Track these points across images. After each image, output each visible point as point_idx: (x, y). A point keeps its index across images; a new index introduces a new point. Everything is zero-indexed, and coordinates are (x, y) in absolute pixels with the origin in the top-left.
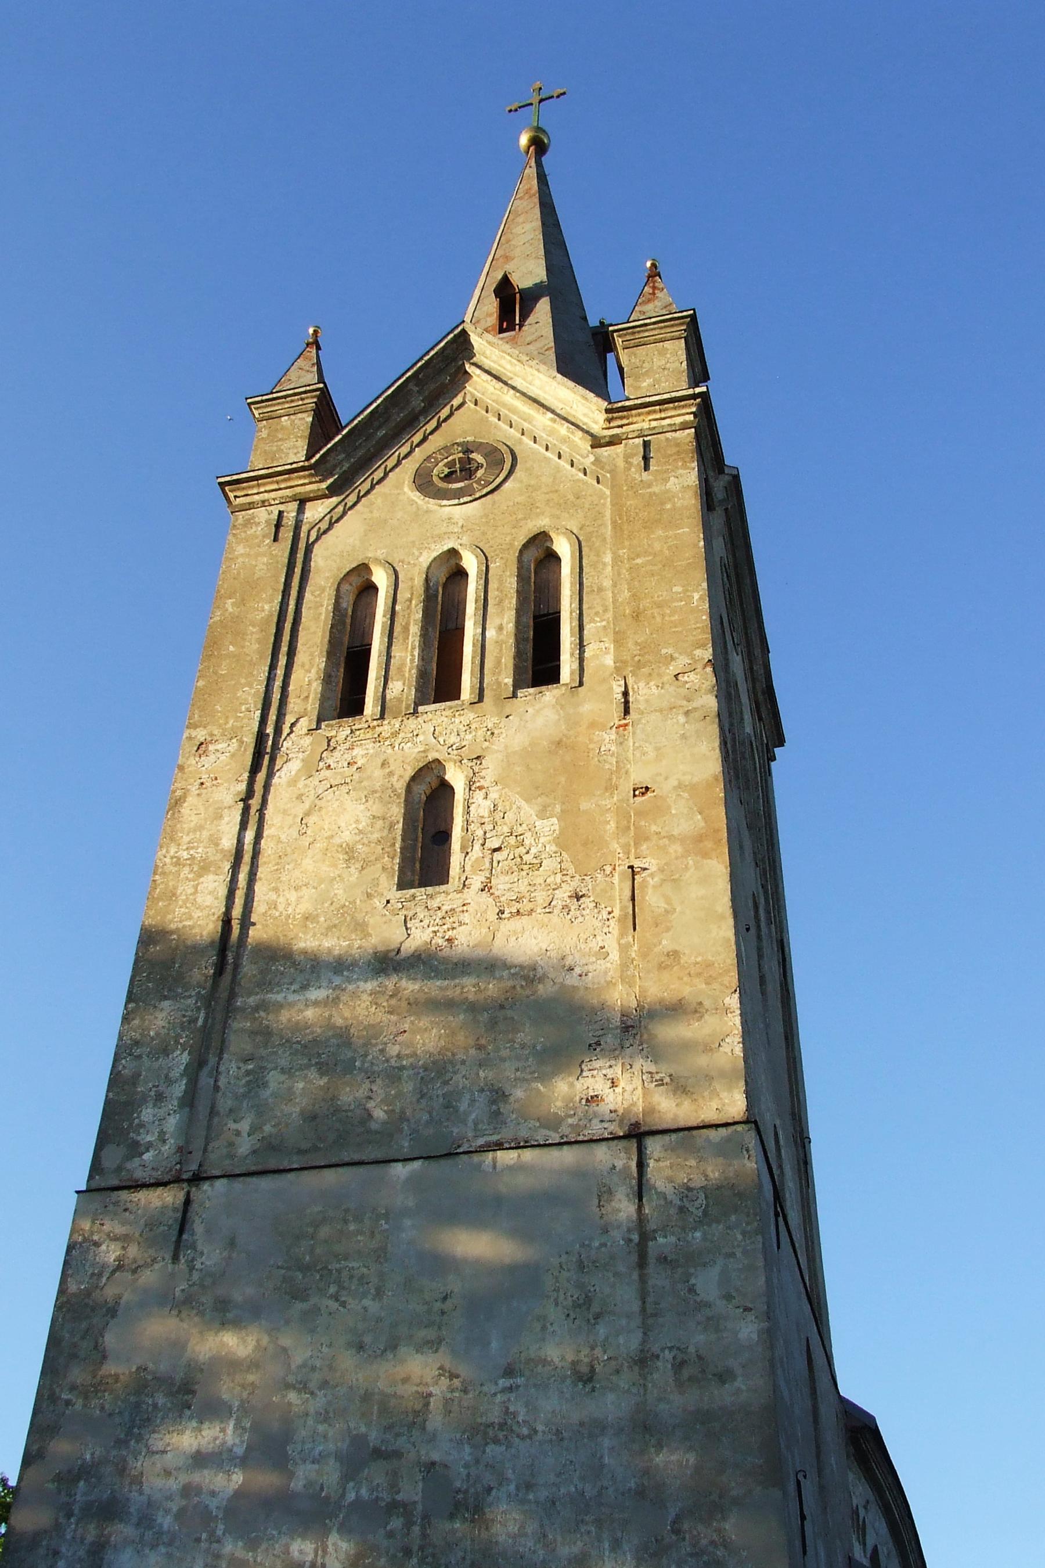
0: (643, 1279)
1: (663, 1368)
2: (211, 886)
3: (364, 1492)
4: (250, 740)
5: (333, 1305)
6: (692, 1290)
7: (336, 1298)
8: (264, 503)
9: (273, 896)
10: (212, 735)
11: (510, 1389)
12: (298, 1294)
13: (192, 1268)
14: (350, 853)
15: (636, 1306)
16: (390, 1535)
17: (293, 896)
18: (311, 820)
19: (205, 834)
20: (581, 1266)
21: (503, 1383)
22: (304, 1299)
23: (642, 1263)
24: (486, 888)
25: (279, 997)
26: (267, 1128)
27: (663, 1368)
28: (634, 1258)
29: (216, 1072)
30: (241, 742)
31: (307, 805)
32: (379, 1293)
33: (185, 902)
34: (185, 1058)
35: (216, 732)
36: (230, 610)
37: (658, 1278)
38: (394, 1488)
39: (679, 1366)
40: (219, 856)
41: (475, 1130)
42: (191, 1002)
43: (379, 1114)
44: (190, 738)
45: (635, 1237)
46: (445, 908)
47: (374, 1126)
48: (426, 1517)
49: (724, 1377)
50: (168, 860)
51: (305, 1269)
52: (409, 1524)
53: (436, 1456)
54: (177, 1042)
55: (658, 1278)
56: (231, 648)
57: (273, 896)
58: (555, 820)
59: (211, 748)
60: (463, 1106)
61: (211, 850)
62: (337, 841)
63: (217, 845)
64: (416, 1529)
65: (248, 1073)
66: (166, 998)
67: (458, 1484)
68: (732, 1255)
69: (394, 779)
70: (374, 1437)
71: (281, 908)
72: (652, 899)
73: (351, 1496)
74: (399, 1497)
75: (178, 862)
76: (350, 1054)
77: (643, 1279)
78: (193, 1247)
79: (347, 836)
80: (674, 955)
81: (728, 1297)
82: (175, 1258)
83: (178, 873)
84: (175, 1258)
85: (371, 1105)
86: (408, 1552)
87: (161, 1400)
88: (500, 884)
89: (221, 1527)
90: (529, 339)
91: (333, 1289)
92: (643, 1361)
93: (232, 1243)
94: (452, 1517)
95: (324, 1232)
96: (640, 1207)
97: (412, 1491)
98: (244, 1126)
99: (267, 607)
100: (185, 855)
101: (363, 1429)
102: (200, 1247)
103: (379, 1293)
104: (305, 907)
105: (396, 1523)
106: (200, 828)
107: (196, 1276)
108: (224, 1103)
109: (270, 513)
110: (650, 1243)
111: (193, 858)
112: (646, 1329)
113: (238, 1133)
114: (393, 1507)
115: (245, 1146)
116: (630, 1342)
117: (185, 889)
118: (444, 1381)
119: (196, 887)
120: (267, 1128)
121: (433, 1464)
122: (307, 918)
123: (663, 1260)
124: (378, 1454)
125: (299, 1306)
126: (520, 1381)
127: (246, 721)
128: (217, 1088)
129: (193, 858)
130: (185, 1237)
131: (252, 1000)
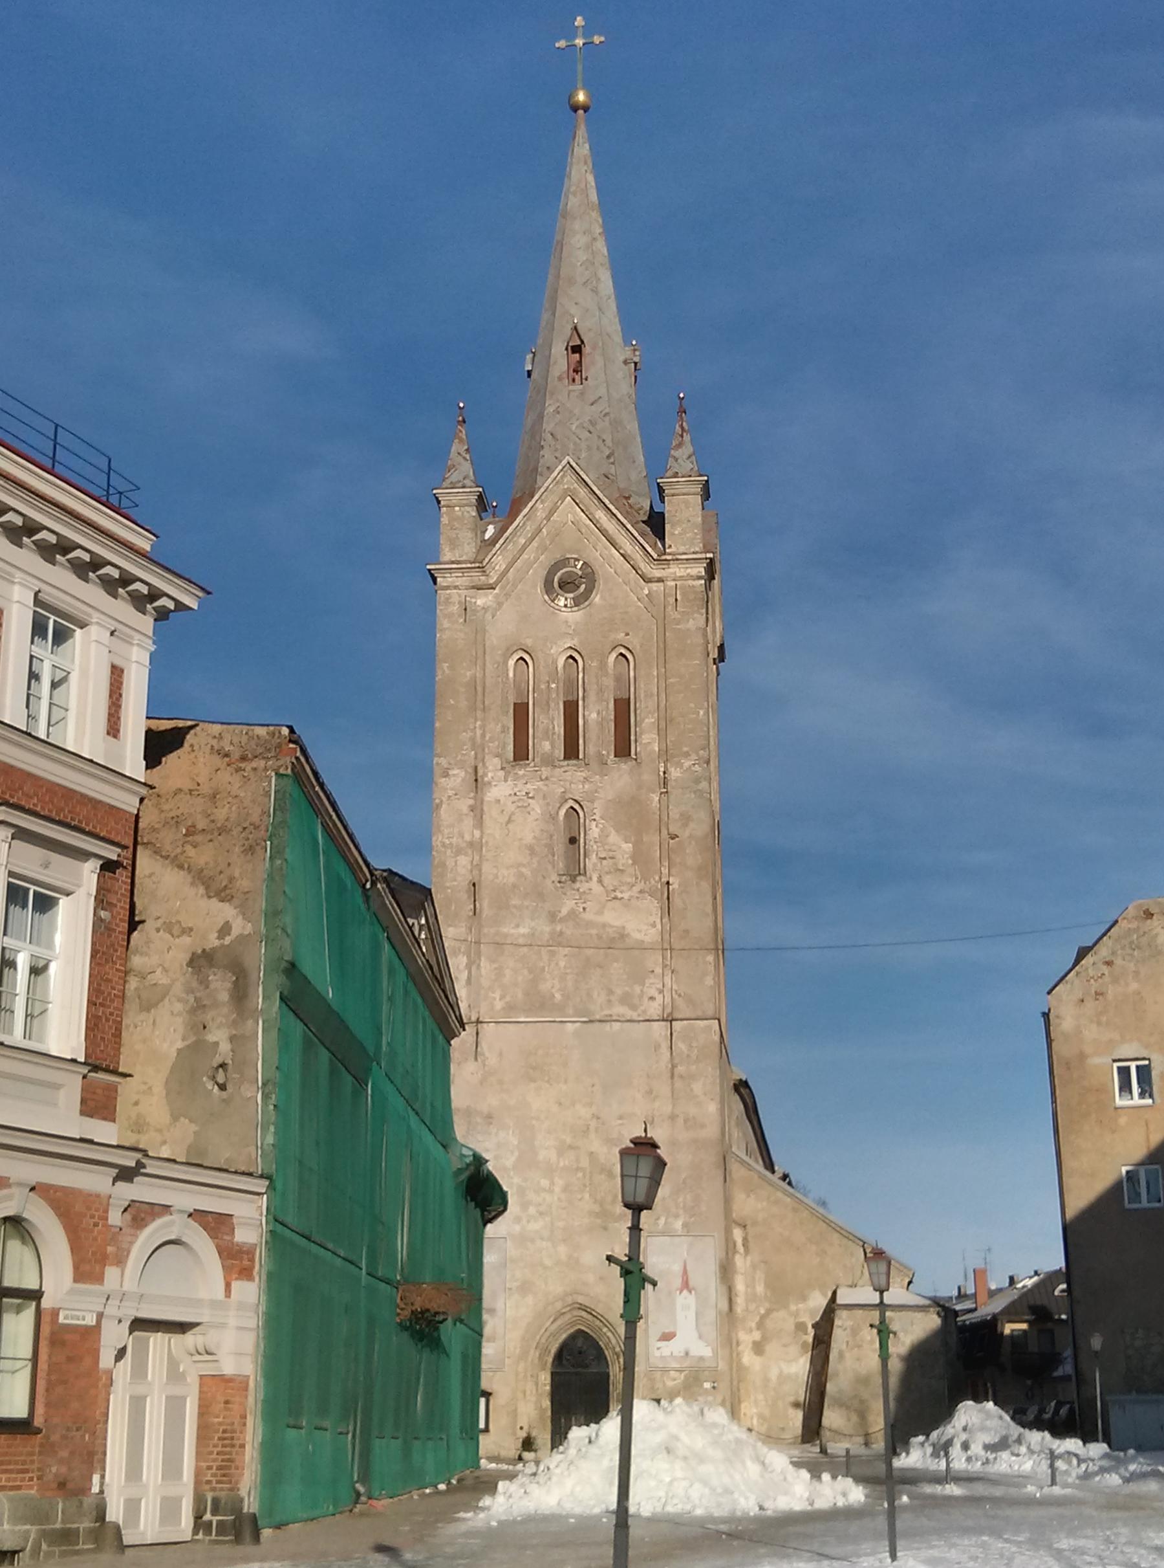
0: (673, 1084)
1: (680, 1121)
2: (464, 863)
3: (567, 1163)
4: (471, 770)
5: (548, 1086)
6: (692, 1090)
7: (548, 1082)
8: (456, 587)
9: (495, 871)
10: (450, 764)
11: (621, 1125)
12: (533, 1080)
13: (484, 1065)
14: (532, 850)
15: (670, 1095)
16: (578, 1179)
17: (506, 872)
18: (510, 826)
19: (456, 830)
20: (648, 1076)
21: (620, 1122)
22: (535, 1081)
23: (672, 1076)
24: (600, 881)
25: (505, 930)
26: (508, 999)
27: (680, 1121)
28: (669, 1075)
29: (479, 965)
30: (466, 771)
31: (507, 818)
32: (566, 1082)
33: (452, 870)
34: (465, 960)
35: (452, 762)
36: (447, 671)
37: (678, 1084)
38: (578, 1160)
39: (685, 1121)
40: (464, 845)
41: (601, 1007)
42: (463, 929)
43: (558, 996)
44: (438, 764)
45: (670, 1066)
46: (581, 890)
47: (556, 1001)
48: (591, 1173)
49: (703, 1126)
50: (439, 844)
51: (534, 1068)
52: (584, 1176)
53: (593, 1149)
54: (460, 950)
55: (678, 1084)
56: (452, 702)
57: (495, 871)
58: (631, 845)
59: (451, 772)
60: (595, 995)
61: (460, 840)
62: (524, 842)
63: (463, 837)
64: (588, 1177)
65: (496, 969)
66: (450, 926)
67: (603, 1161)
68: (706, 1077)
69: (550, 808)
70: (569, 1140)
71: (500, 878)
72: (677, 901)
73: (562, 1164)
74: (581, 1165)
75: (444, 845)
76: (542, 964)
77: (673, 1084)
78: (483, 1055)
79: (529, 838)
80: (687, 931)
81: (705, 1094)
82: (476, 1059)
83: (445, 853)
84: (476, 1059)
85: (554, 991)
86: (585, 1186)
87: (479, 1120)
88: (607, 880)
89: (512, 1173)
90: (592, 399)
91: (546, 1079)
92: (673, 1117)
93: (501, 1054)
94: (601, 1173)
95: (540, 1052)
96: (672, 1053)
97: (585, 1163)
98: (497, 995)
99: (468, 674)
100: (447, 842)
101: (564, 1137)
102: (487, 1054)
103: (566, 1082)
104: (512, 880)
105: (580, 1175)
106: (452, 826)
107: (486, 1068)
108: (485, 983)
109: (460, 596)
110: (675, 1069)
111: (451, 844)
112: (674, 1106)
113: (495, 999)
114: (578, 1169)
115: (499, 1005)
116: (668, 1109)
117: (450, 863)
118: (595, 1120)
119: (456, 862)
120: (508, 999)
121: (592, 1153)
122: (514, 886)
123: (681, 1077)
124: (571, 1147)
125: (533, 1085)
126: (625, 1121)
127: (466, 757)
128: (481, 976)
129: (451, 844)
130: (479, 1049)
131: (492, 931)
